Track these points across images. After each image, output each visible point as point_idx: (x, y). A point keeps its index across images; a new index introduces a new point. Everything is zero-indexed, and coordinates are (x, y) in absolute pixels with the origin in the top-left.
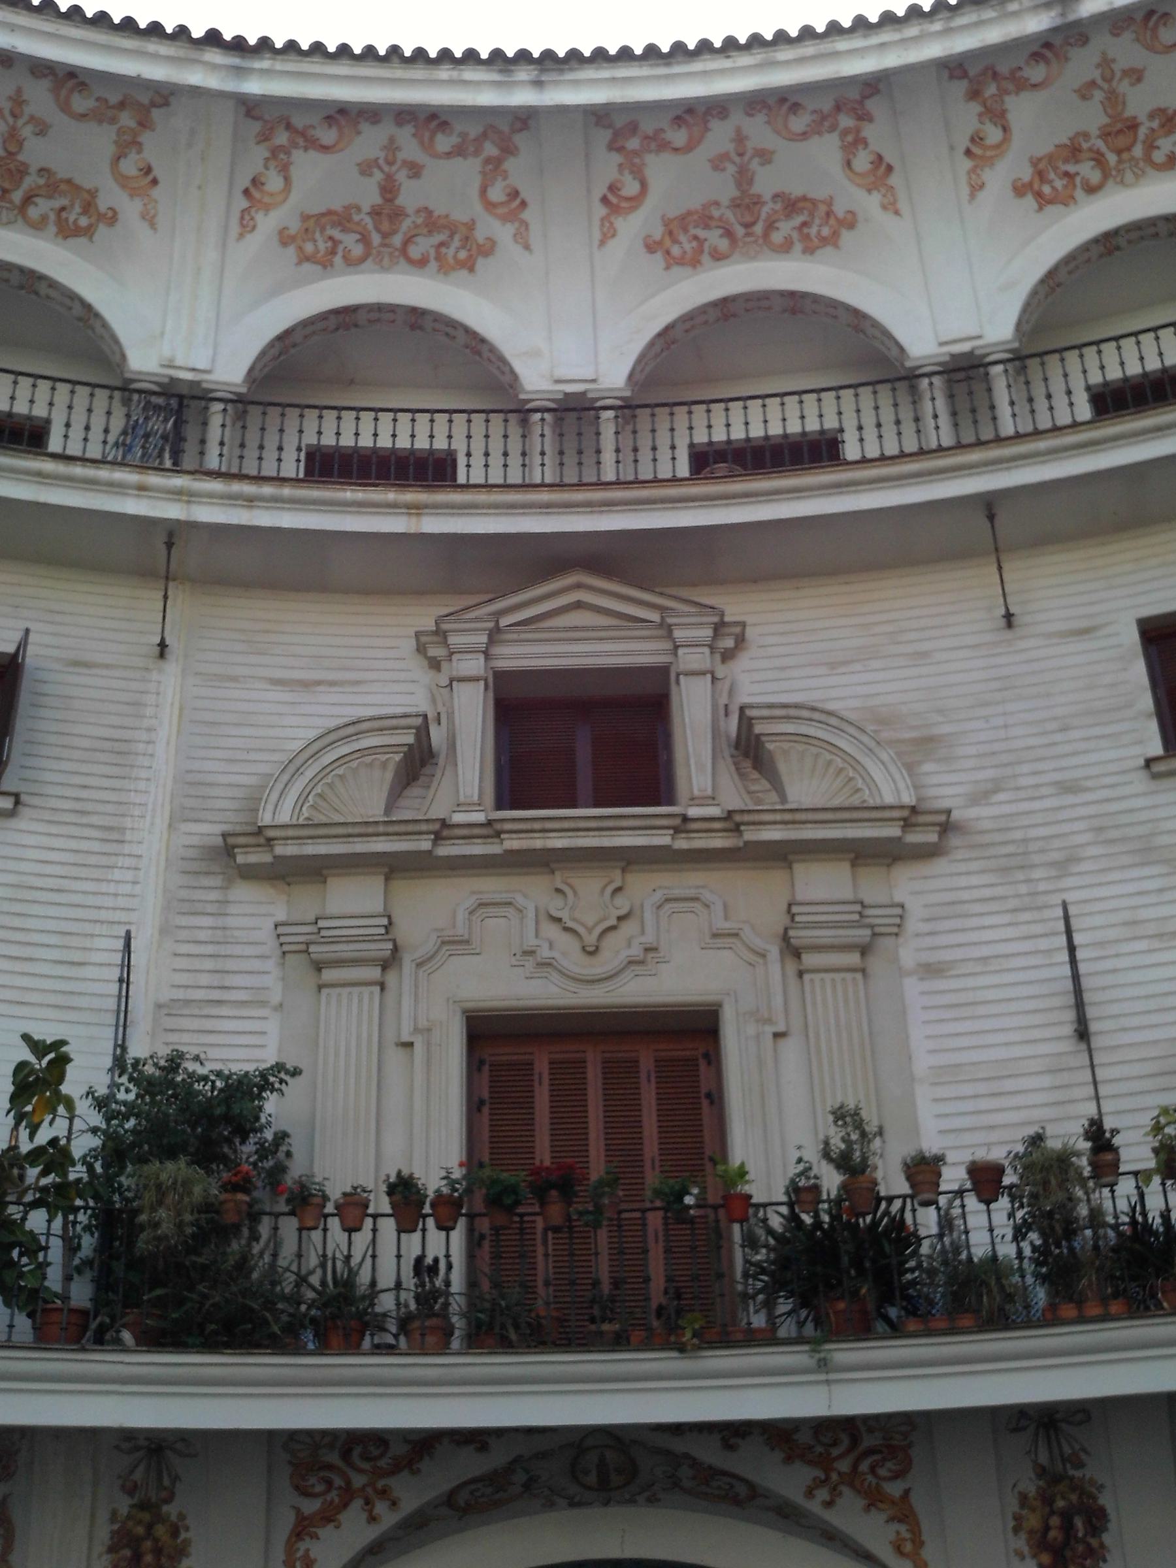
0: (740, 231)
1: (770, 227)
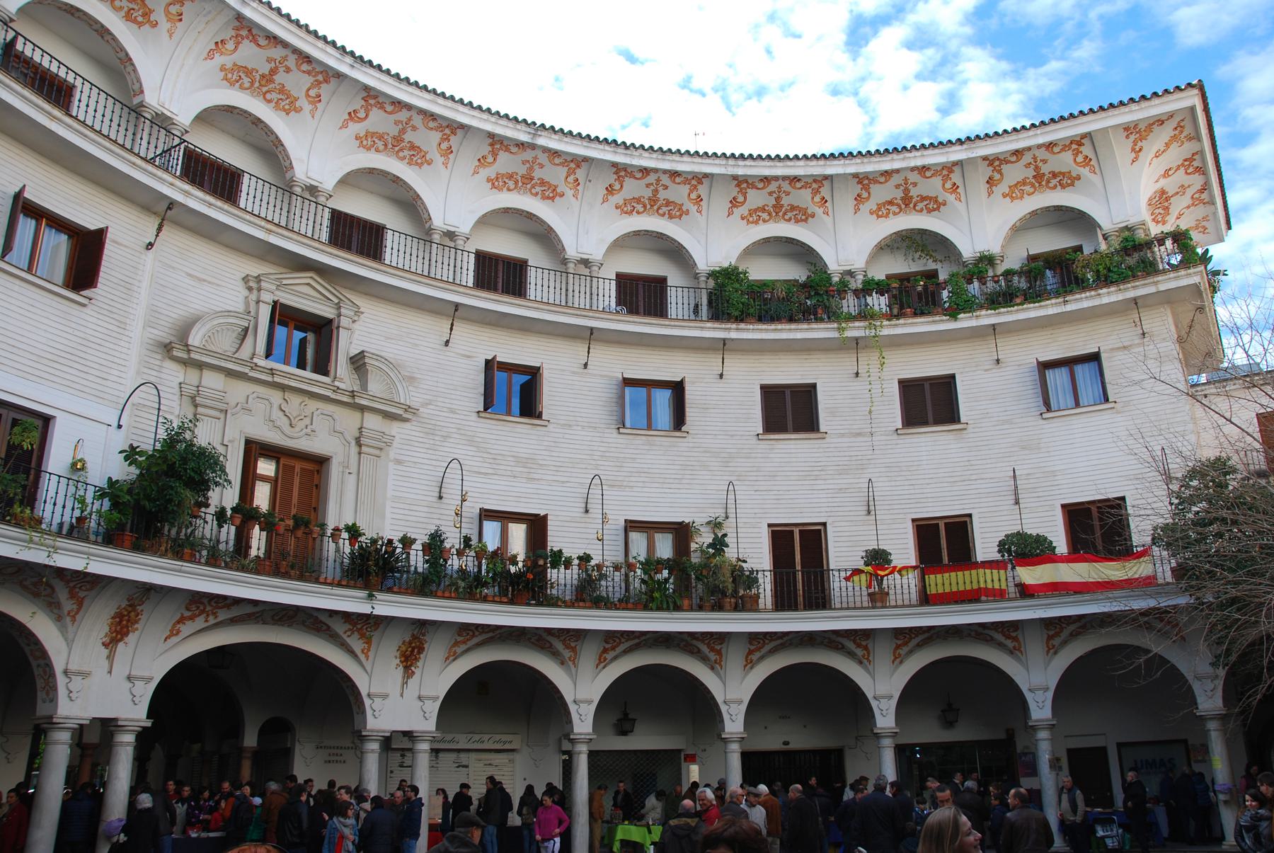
1: (401, 150)
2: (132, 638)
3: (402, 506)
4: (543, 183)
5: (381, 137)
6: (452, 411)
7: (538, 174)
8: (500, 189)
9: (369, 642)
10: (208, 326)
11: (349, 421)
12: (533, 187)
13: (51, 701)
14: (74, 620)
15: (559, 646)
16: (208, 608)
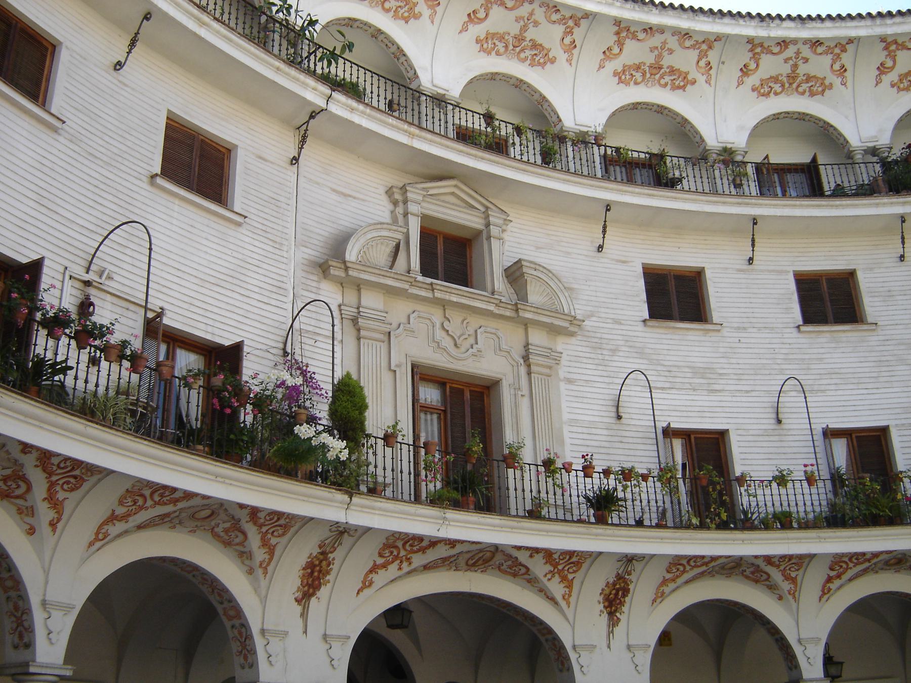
0: (511, 47)
1: (522, 50)
2: (324, 592)
3: (580, 430)
4: (672, 71)
5: (501, 38)
6: (617, 322)
7: (667, 61)
8: (628, 84)
9: (570, 586)
10: (362, 241)
11: (512, 338)
12: (662, 77)
13: (251, 666)
14: (265, 573)
15: (776, 575)
16: (403, 553)
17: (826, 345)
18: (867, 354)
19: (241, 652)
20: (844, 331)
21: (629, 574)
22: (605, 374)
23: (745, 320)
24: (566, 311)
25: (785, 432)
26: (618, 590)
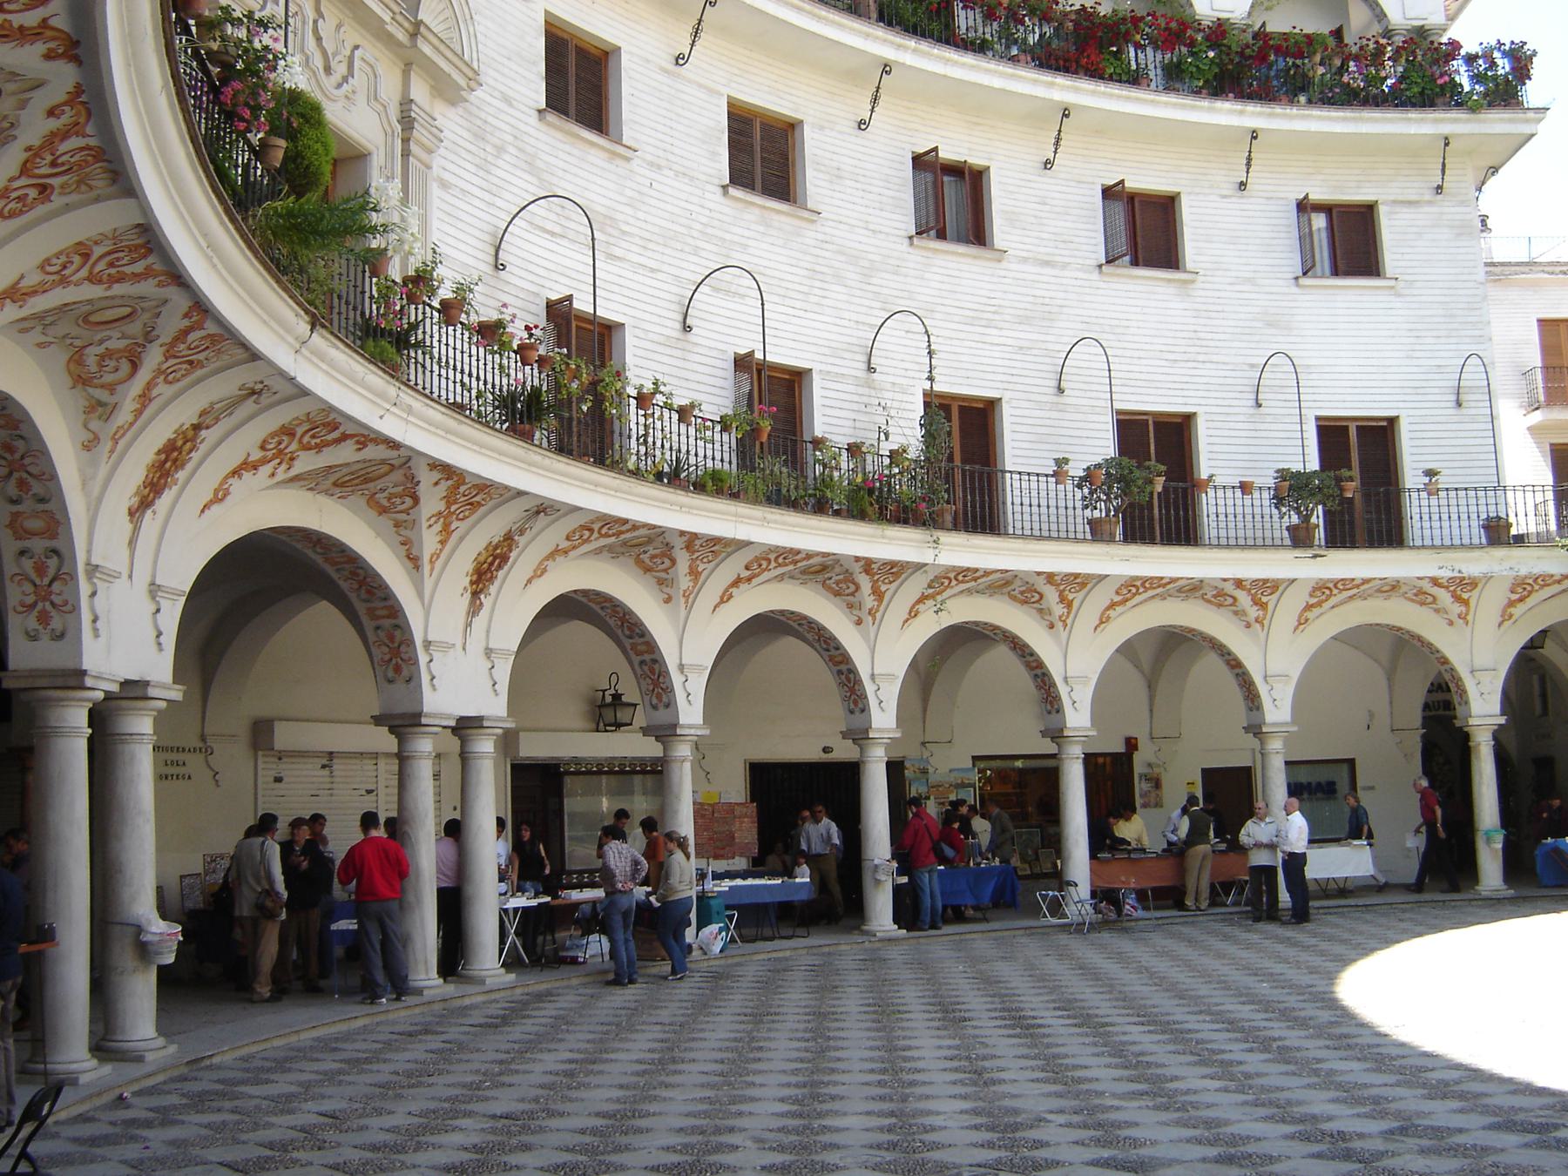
6: (507, 100)
17: (753, 227)
18: (800, 256)
19: (34, 605)
20: (779, 212)
21: (522, 532)
22: (485, 185)
23: (661, 153)
24: (466, 57)
25: (689, 347)
26: (495, 558)
